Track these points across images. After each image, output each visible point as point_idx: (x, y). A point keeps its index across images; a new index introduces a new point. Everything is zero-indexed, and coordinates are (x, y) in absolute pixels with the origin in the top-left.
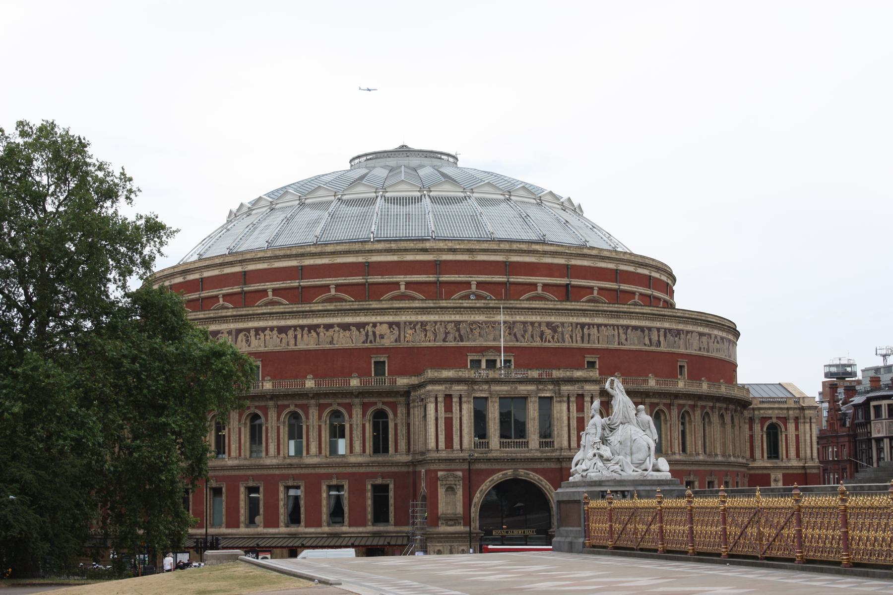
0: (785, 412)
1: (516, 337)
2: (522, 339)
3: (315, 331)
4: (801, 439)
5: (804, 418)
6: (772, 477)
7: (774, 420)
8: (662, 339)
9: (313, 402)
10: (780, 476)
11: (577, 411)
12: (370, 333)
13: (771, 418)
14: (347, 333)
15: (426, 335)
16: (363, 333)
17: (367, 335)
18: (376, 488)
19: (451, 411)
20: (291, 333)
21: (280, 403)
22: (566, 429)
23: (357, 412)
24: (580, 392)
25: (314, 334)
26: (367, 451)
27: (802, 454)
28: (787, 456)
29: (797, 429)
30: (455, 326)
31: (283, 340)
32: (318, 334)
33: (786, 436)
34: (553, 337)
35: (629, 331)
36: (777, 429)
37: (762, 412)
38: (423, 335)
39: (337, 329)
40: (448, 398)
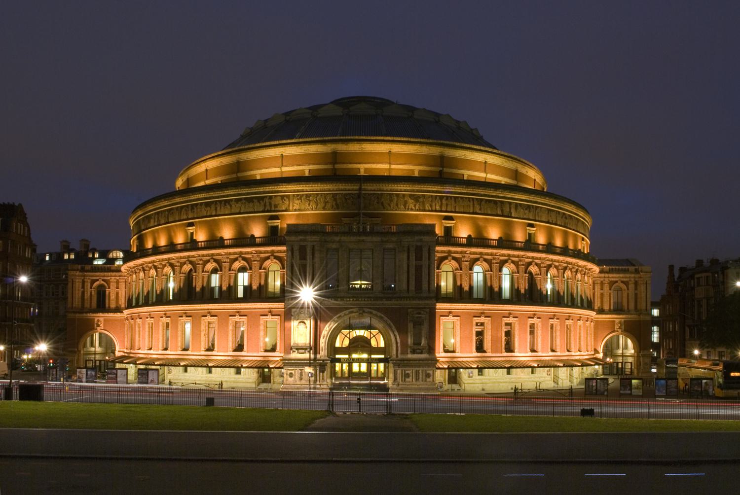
1: (382, 204)
2: (389, 208)
3: (229, 204)
8: (513, 211)
11: (416, 260)
12: (268, 204)
14: (251, 205)
15: (309, 204)
16: (262, 204)
17: (265, 206)
19: (305, 259)
20: (213, 207)
22: (405, 275)
24: (419, 244)
25: (228, 206)
30: (333, 196)
31: (208, 212)
32: (231, 206)
34: (415, 206)
35: (483, 203)
38: (307, 204)
39: (244, 201)
40: (303, 249)
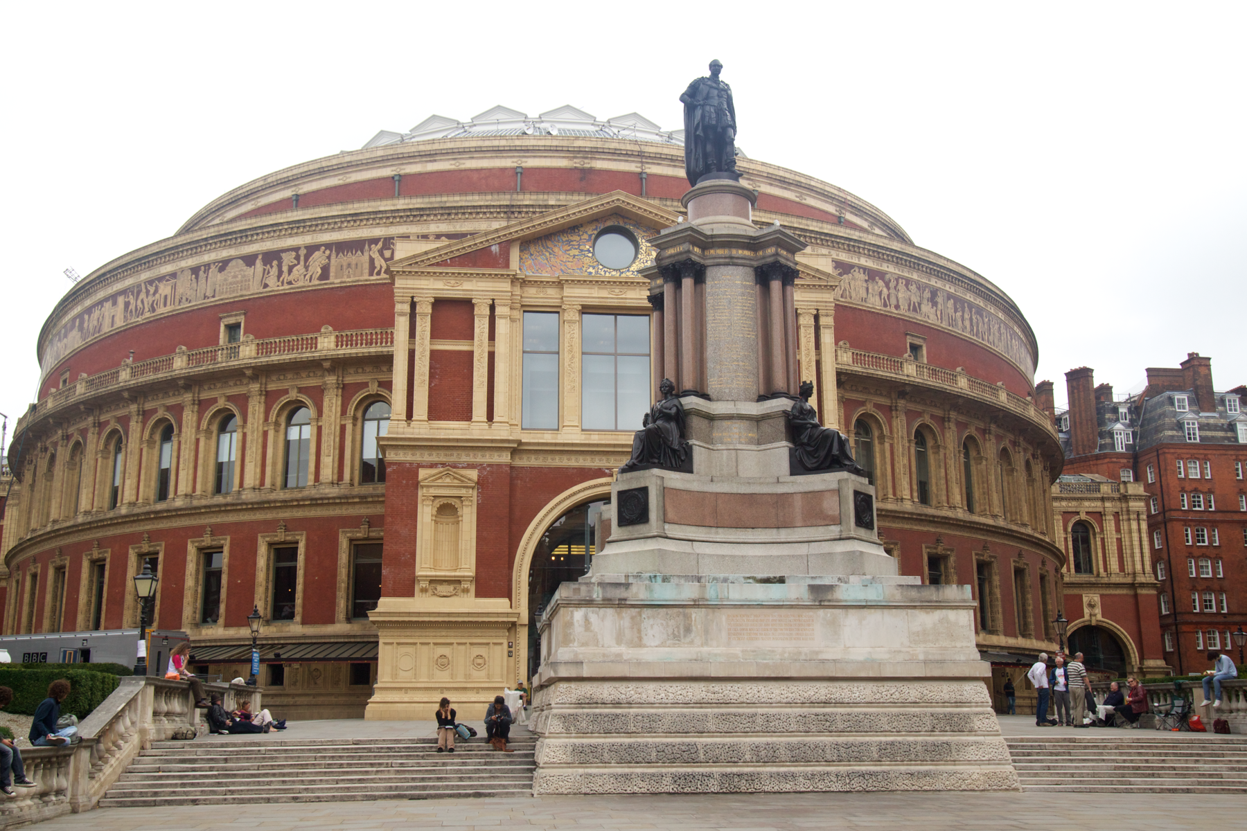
0: (1099, 504)
4: (1126, 542)
5: (1128, 511)
6: (1085, 600)
7: (1083, 516)
9: (255, 387)
10: (1096, 599)
13: (1078, 513)
18: (358, 548)
21: (205, 395)
23: (332, 403)
26: (347, 476)
27: (1129, 569)
28: (1106, 570)
29: (1118, 530)
33: (1103, 539)
36: (1087, 531)
37: (1064, 503)
